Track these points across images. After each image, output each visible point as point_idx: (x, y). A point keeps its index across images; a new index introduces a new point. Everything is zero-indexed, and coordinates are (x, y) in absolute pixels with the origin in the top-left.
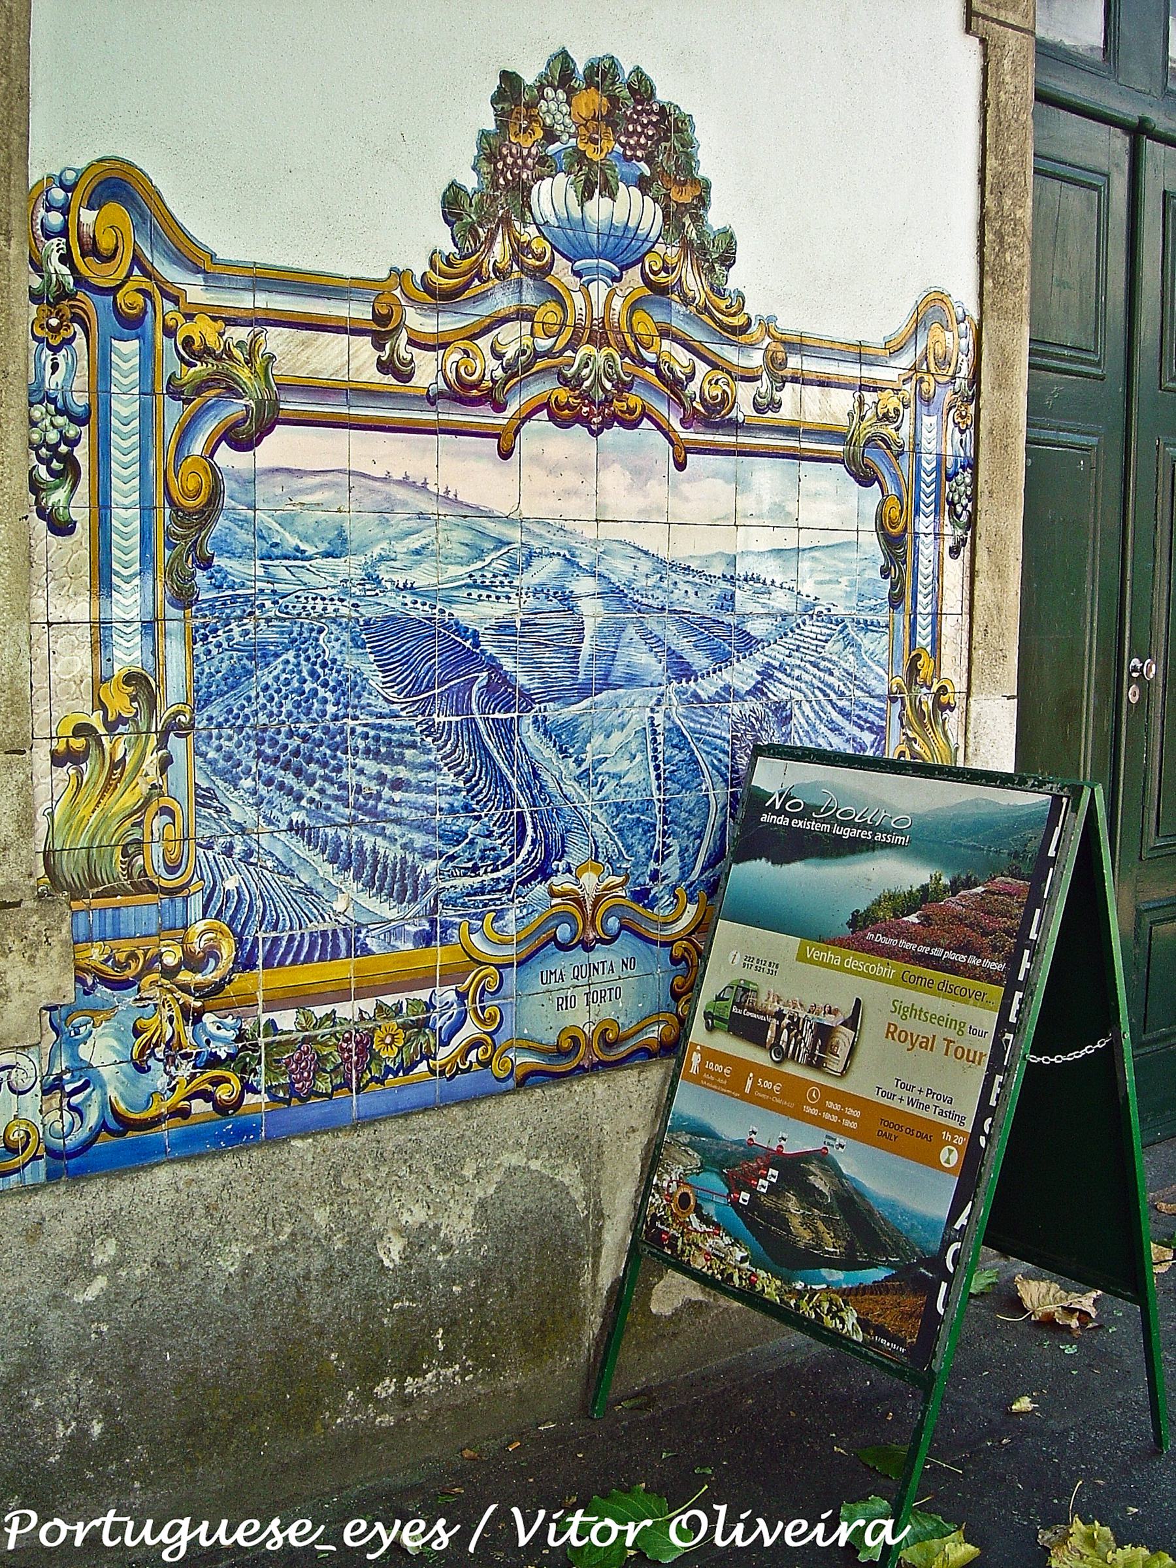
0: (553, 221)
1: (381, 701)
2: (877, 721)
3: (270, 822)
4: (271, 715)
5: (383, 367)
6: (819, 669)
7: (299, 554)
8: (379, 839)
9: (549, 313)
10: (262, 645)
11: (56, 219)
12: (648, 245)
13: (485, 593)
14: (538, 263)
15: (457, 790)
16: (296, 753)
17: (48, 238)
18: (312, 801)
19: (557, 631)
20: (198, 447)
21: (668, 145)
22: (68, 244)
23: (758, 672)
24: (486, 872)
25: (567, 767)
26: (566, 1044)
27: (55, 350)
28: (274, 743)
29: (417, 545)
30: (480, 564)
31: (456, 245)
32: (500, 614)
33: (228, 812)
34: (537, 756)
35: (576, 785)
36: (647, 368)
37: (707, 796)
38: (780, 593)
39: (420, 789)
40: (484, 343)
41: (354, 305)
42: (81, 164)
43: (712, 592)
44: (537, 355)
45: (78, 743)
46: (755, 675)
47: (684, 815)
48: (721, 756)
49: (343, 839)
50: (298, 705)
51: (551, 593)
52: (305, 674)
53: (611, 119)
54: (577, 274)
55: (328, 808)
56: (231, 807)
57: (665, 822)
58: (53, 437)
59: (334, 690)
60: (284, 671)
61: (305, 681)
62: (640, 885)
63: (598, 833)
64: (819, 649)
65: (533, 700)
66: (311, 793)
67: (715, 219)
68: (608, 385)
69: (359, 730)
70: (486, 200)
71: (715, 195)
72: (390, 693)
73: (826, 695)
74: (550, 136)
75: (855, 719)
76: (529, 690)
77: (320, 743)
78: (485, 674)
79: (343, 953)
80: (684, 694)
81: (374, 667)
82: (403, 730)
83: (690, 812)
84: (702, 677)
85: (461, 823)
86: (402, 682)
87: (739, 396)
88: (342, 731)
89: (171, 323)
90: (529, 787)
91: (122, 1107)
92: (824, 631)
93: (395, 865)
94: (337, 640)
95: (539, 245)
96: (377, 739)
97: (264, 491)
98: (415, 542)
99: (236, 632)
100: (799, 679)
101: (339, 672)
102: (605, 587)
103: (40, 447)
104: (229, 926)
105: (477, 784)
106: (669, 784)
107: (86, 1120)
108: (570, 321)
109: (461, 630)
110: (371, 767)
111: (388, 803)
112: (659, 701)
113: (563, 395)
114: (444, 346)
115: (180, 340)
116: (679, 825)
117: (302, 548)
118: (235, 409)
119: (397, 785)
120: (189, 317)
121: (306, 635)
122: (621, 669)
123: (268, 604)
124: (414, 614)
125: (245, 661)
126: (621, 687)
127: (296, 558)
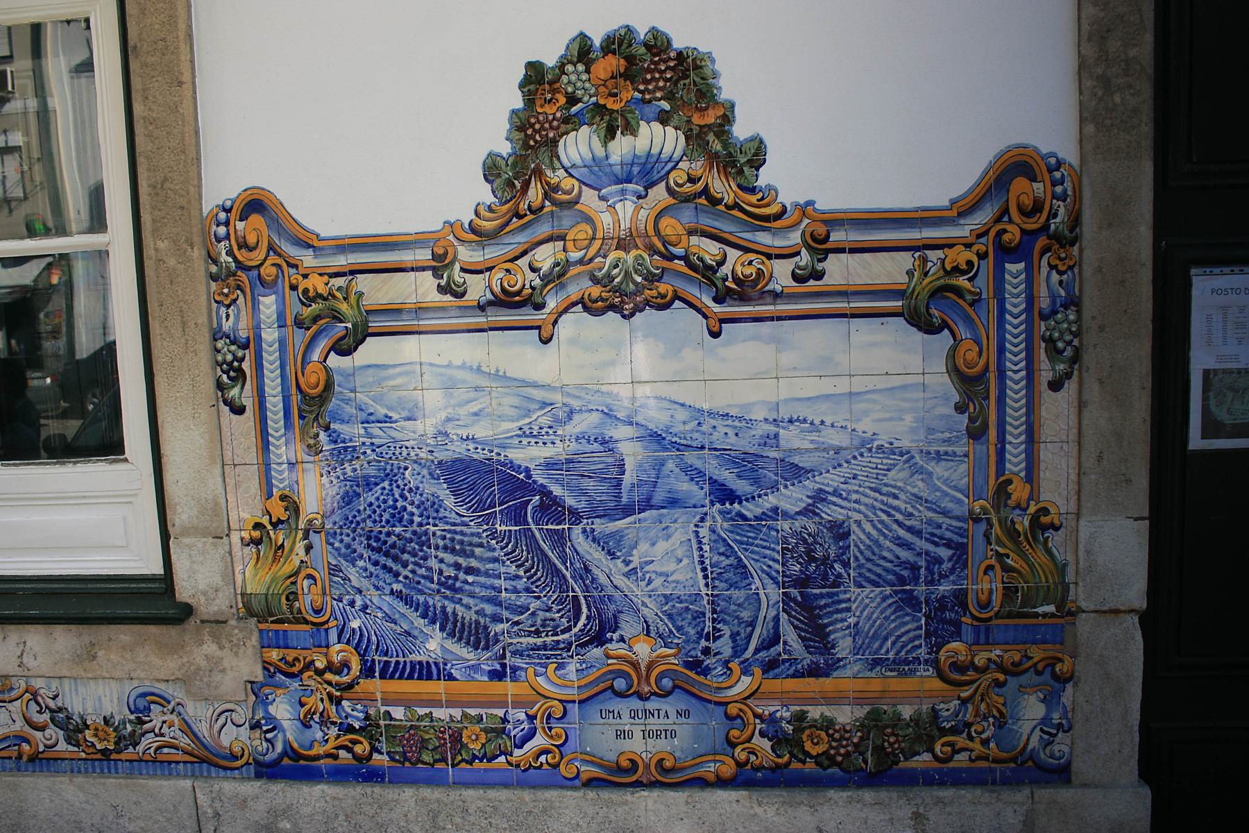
0: (579, 162)
1: (454, 515)
2: (956, 538)
3: (377, 588)
4: (375, 521)
5: (442, 290)
6: (881, 494)
7: (388, 419)
8: (458, 606)
10: (366, 478)
12: (670, 165)
13: (533, 441)
14: (567, 197)
15: (517, 577)
16: (393, 546)
18: (406, 577)
19: (600, 466)
20: (316, 356)
21: (687, 81)
23: (808, 497)
24: (547, 635)
25: (615, 565)
26: (625, 764)
27: (228, 306)
28: (377, 539)
29: (475, 409)
30: (527, 420)
31: (496, 196)
32: (548, 455)
33: (349, 580)
34: (588, 557)
35: (625, 579)
36: (676, 261)
37: (758, 594)
38: (831, 431)
39: (487, 574)
41: (418, 251)
42: (234, 196)
43: (754, 433)
45: (256, 534)
46: (804, 498)
47: (733, 607)
48: (771, 563)
49: (431, 603)
50: (393, 516)
51: (592, 438)
52: (397, 496)
53: (630, 74)
55: (419, 583)
56: (352, 578)
57: (714, 611)
58: (229, 357)
59: (418, 507)
60: (382, 494)
61: (396, 501)
62: (691, 657)
63: (648, 615)
64: (880, 477)
65: (582, 517)
66: (405, 572)
67: (741, 130)
68: (639, 279)
69: (439, 533)
70: (519, 160)
72: (462, 511)
73: (889, 515)
74: (572, 100)
75: (928, 536)
76: (577, 509)
77: (411, 541)
78: (538, 497)
79: (435, 676)
80: (728, 513)
81: (448, 492)
82: (472, 534)
83: (739, 605)
84: (747, 500)
85: (523, 599)
86: (469, 502)
87: (775, 271)
88: (426, 533)
89: (294, 282)
90: (581, 578)
91: (295, 745)
92: (885, 461)
93: (471, 624)
94: (419, 474)
95: (568, 183)
96: (452, 540)
97: (359, 381)
98: (475, 407)
99: (349, 469)
100: (856, 502)
101: (421, 495)
102: (641, 432)
103: (222, 364)
104: (356, 649)
105: (536, 573)
106: (717, 583)
108: (599, 235)
109: (512, 465)
110: (449, 558)
111: (463, 582)
112: (702, 520)
113: (596, 291)
114: (490, 269)
115: (300, 290)
116: (729, 615)
117: (390, 415)
119: (470, 571)
121: (396, 471)
122: (663, 494)
123: (369, 452)
124: (475, 456)
125: (355, 488)
126: (663, 507)
127: (386, 422)
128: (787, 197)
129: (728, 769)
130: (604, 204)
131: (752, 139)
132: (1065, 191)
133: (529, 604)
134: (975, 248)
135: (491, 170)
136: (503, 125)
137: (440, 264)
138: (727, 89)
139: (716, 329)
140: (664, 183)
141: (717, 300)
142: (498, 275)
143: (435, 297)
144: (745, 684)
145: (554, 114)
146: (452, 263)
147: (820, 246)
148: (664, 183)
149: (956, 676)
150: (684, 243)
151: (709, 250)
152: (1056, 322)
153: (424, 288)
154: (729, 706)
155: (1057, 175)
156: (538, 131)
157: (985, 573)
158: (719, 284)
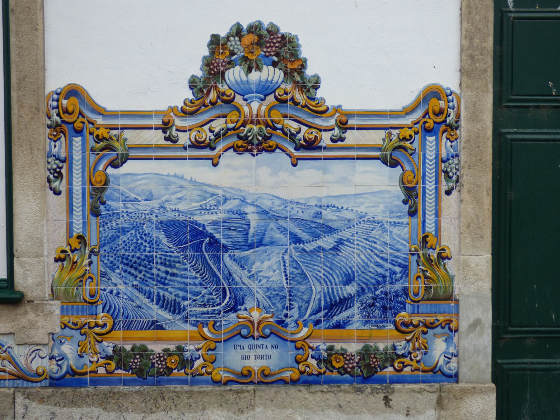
1: (166, 247)
2: (403, 263)
3: (125, 284)
4: (126, 250)
5: (166, 139)
6: (369, 241)
7: (136, 200)
8: (166, 293)
9: (234, 116)
10: (123, 228)
11: (55, 104)
12: (277, 86)
13: (207, 212)
14: (228, 98)
15: (196, 278)
16: (135, 262)
17: (53, 109)
18: (141, 278)
19: (238, 225)
20: (101, 168)
21: (286, 48)
22: (59, 111)
23: (335, 242)
24: (209, 307)
25: (244, 273)
26: (245, 372)
27: (55, 141)
28: (127, 259)
29: (180, 196)
30: (204, 202)
31: (194, 96)
32: (214, 219)
33: (111, 279)
34: (231, 268)
35: (249, 280)
36: (278, 131)
37: (311, 287)
38: (346, 212)
39: (181, 277)
40: (206, 128)
42: (62, 87)
43: (311, 211)
44: (228, 130)
46: (333, 242)
47: (299, 294)
48: (317, 273)
49: (152, 291)
50: (136, 247)
51: (235, 212)
52: (138, 237)
53: (259, 44)
54: (245, 100)
55: (147, 281)
56: (112, 278)
57: (291, 295)
58: (55, 166)
59: (149, 243)
60: (131, 236)
61: (138, 240)
62: (280, 318)
63: (259, 297)
64: (368, 233)
65: (228, 249)
66: (140, 276)
67: (309, 72)
68: (260, 138)
69: (158, 256)
70: (206, 80)
71: (309, 64)
72: (171, 245)
73: (372, 251)
74: (232, 54)
75: (390, 261)
76: (226, 245)
77: (144, 260)
78: (208, 239)
80: (298, 249)
82: (175, 257)
83: (303, 293)
84: (307, 242)
85: (198, 289)
86: (174, 241)
87: (323, 137)
88: (152, 256)
89: (92, 131)
90: (227, 278)
91: (74, 367)
92: (371, 226)
93: (171, 301)
94: (150, 227)
95: (229, 92)
96: (165, 259)
97: (121, 181)
98: (179, 195)
99: (114, 224)
100: (357, 245)
101: (151, 237)
102: (259, 210)
103: (51, 170)
104: (111, 316)
105: (205, 276)
106: (292, 282)
107: (62, 370)
108: (242, 116)
109: (196, 223)
110: (163, 268)
111: (169, 281)
112: (286, 252)
113: (240, 143)
114: (190, 130)
116: (298, 297)
117: (137, 197)
118: (113, 155)
119: (173, 275)
120: (98, 129)
121: (139, 225)
122: (268, 239)
123: (125, 216)
124: (179, 219)
125: (117, 233)
126: (267, 245)
127: (135, 201)
128: (330, 102)
129: (296, 376)
130: (245, 102)
131: (314, 76)
132: (454, 105)
133: (201, 291)
134: (413, 129)
135: (193, 84)
136: (199, 63)
137: (166, 127)
138: (304, 53)
139: (295, 163)
140: (273, 94)
141: (296, 149)
142: (194, 133)
143: (163, 142)
144: (305, 331)
145: (224, 59)
146: (172, 126)
147: (343, 126)
148: (273, 95)
149: (404, 329)
150: (281, 123)
151: (293, 126)
152: (449, 164)
153: (157, 137)
154: (297, 343)
155: (450, 98)
156: (216, 67)
157: (417, 279)
158: (297, 142)
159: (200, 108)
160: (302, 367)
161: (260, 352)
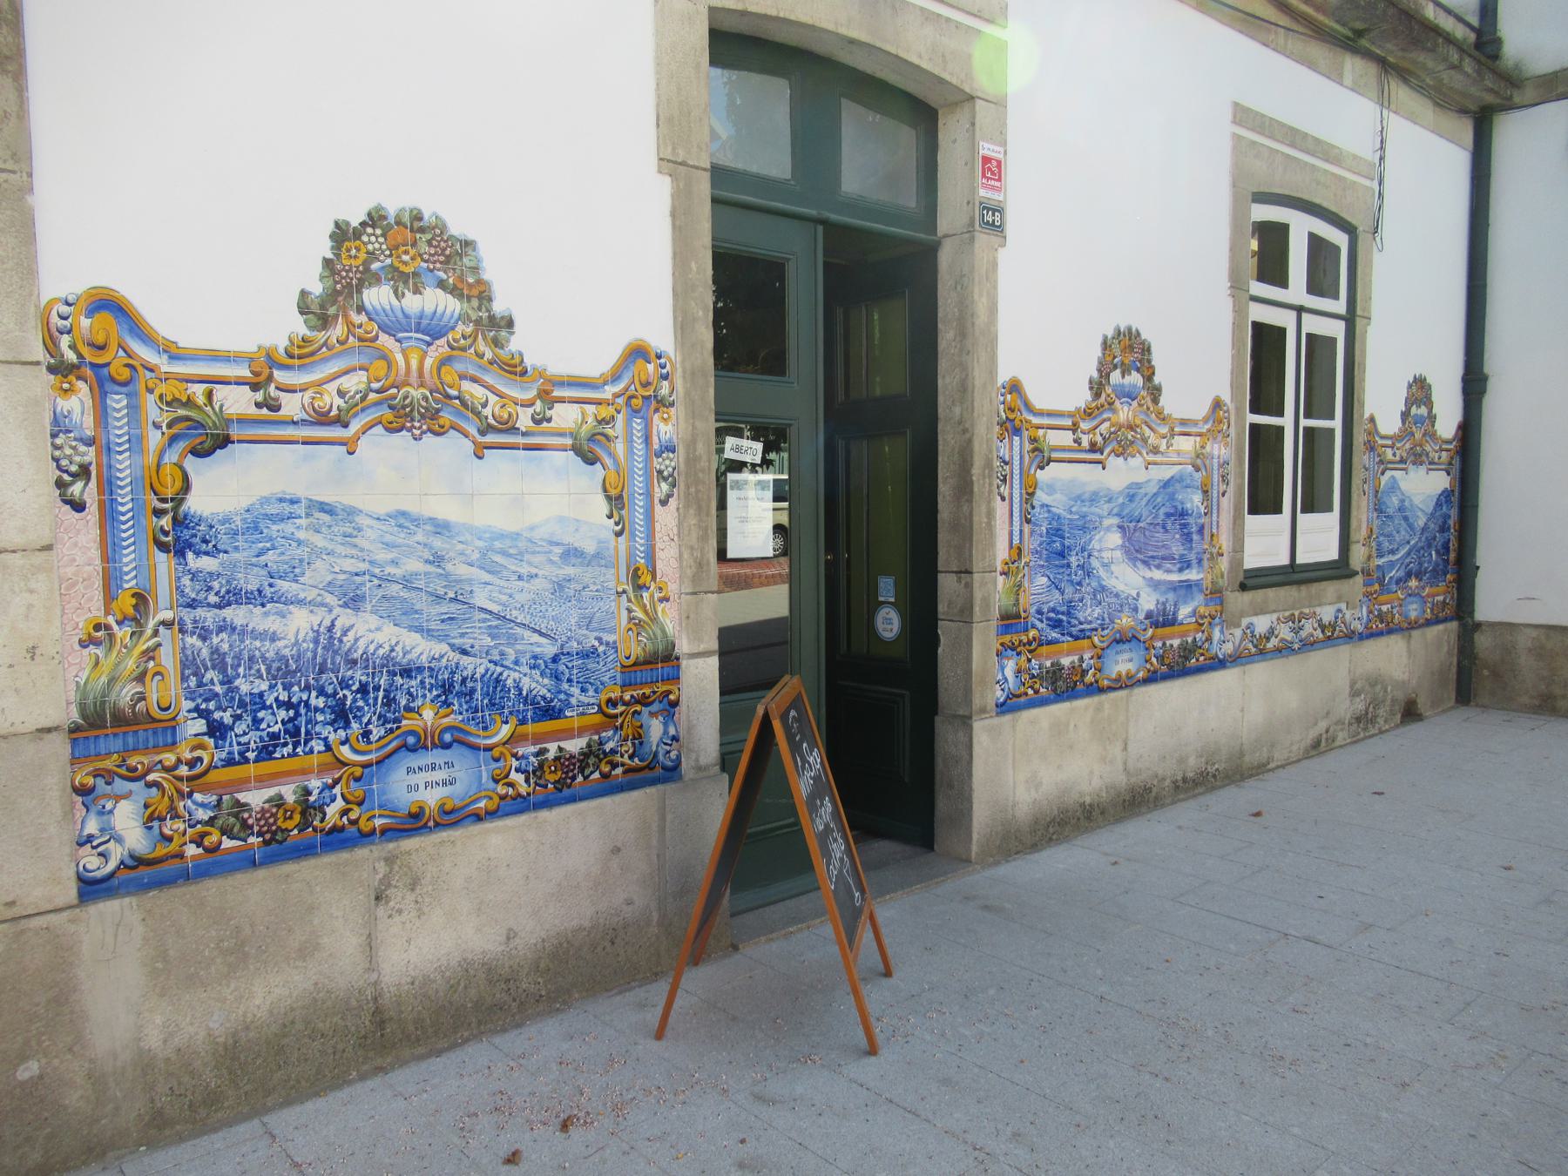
5: (258, 405)
9: (379, 367)
26: (414, 810)
40: (332, 387)
67: (499, 307)
129: (492, 806)
130: (398, 344)
136: (318, 268)
142: (308, 395)
143: (253, 410)
144: (505, 731)
145: (358, 267)
159: (321, 348)
160: (501, 790)
161: (439, 775)
